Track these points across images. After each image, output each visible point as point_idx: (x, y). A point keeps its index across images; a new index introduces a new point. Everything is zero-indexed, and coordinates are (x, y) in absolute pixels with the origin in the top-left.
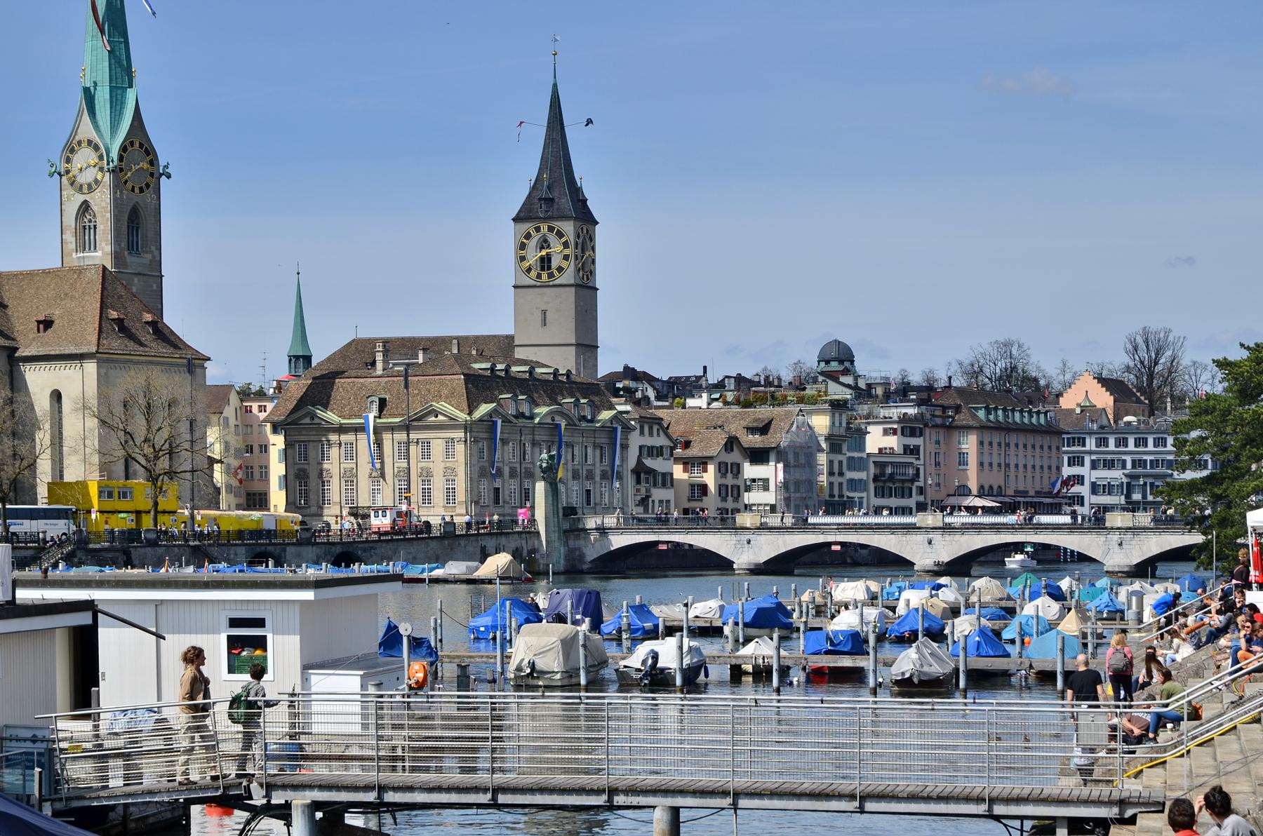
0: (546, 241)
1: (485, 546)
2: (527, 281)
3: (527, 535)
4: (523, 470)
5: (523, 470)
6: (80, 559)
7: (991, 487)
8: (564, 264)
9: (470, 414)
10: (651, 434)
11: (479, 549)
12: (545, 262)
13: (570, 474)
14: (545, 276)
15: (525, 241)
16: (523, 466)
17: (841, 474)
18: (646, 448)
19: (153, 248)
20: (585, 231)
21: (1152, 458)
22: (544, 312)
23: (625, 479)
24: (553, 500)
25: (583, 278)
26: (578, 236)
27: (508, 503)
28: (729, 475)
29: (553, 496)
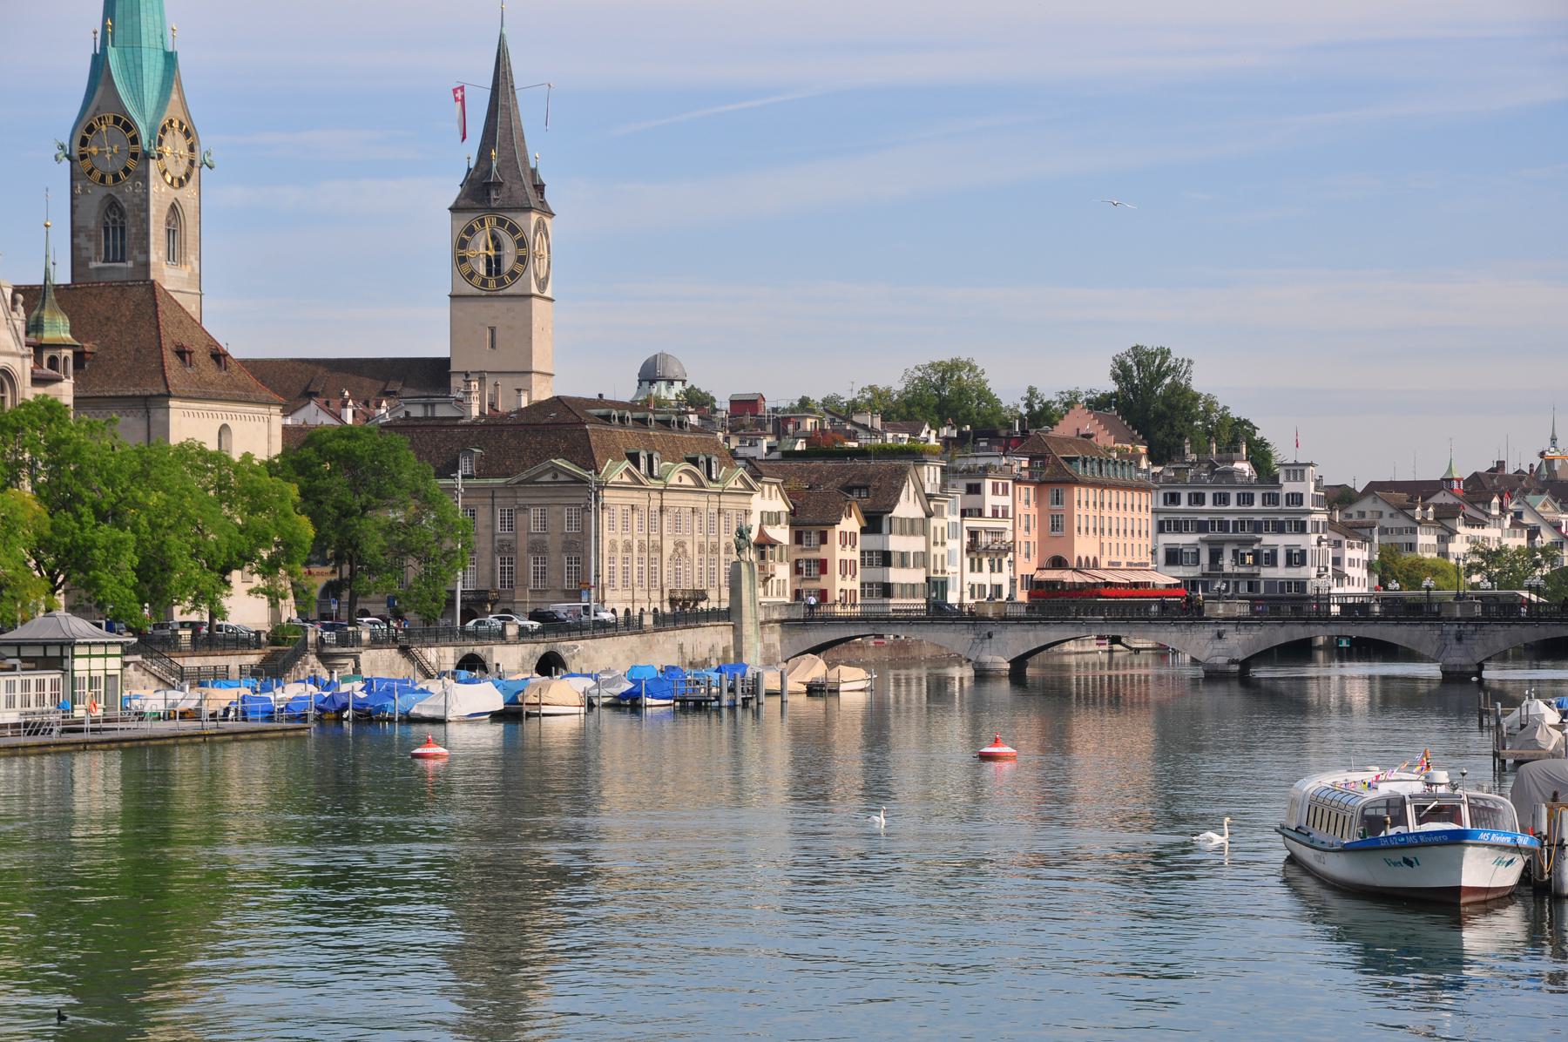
2: (469, 289)
5: (651, 544)
6: (313, 666)
7: (1087, 558)
12: (494, 265)
14: (492, 283)
15: (466, 237)
16: (651, 538)
17: (943, 544)
21: (1235, 518)
22: (493, 330)
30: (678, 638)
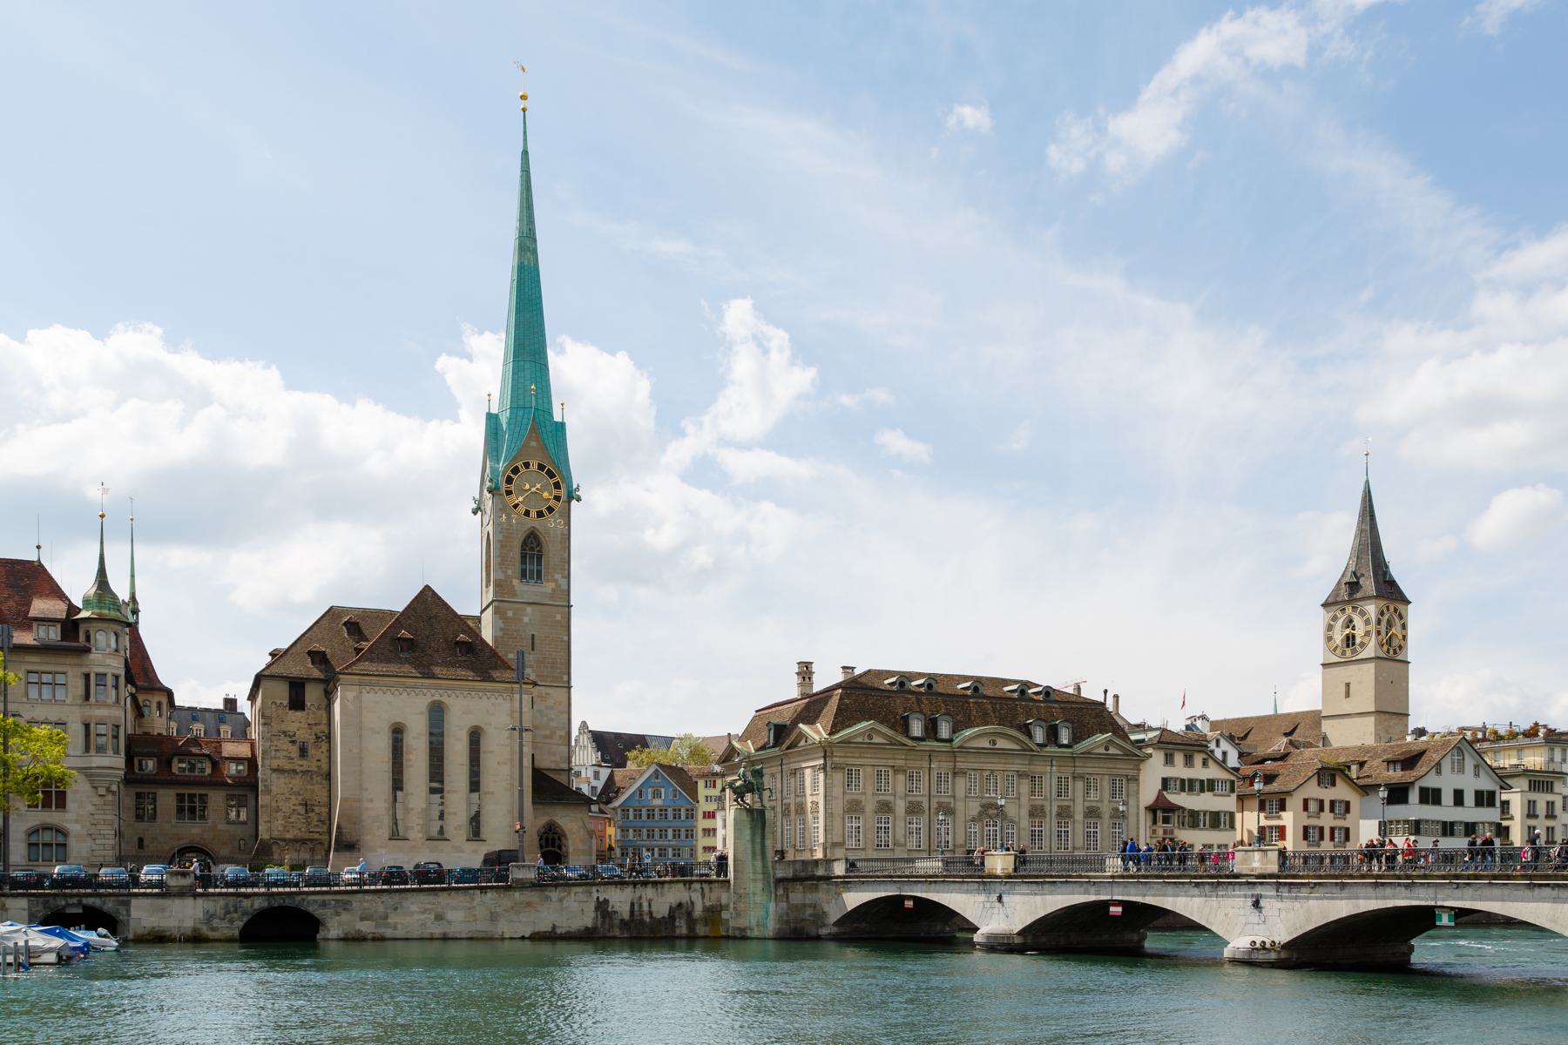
0: (1351, 621)
1: (606, 901)
3: (706, 886)
4: (934, 805)
8: (1365, 641)
9: (829, 734)
10: (1189, 761)
11: (592, 906)
12: (1350, 640)
13: (1025, 812)
15: (1332, 623)
18: (1178, 783)
19: (557, 576)
20: (1392, 609)
22: (1348, 685)
23: (1132, 819)
24: (753, 835)
25: (1388, 651)
26: (1382, 614)
27: (900, 845)
28: (1327, 813)
29: (753, 829)
30: (595, 895)
